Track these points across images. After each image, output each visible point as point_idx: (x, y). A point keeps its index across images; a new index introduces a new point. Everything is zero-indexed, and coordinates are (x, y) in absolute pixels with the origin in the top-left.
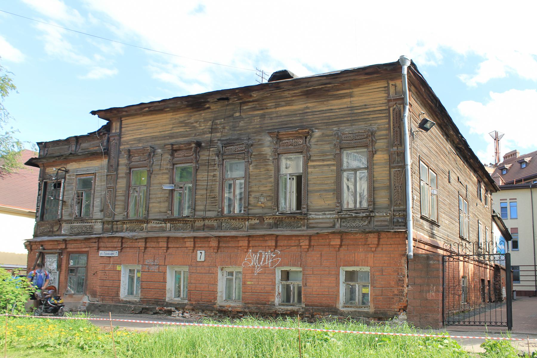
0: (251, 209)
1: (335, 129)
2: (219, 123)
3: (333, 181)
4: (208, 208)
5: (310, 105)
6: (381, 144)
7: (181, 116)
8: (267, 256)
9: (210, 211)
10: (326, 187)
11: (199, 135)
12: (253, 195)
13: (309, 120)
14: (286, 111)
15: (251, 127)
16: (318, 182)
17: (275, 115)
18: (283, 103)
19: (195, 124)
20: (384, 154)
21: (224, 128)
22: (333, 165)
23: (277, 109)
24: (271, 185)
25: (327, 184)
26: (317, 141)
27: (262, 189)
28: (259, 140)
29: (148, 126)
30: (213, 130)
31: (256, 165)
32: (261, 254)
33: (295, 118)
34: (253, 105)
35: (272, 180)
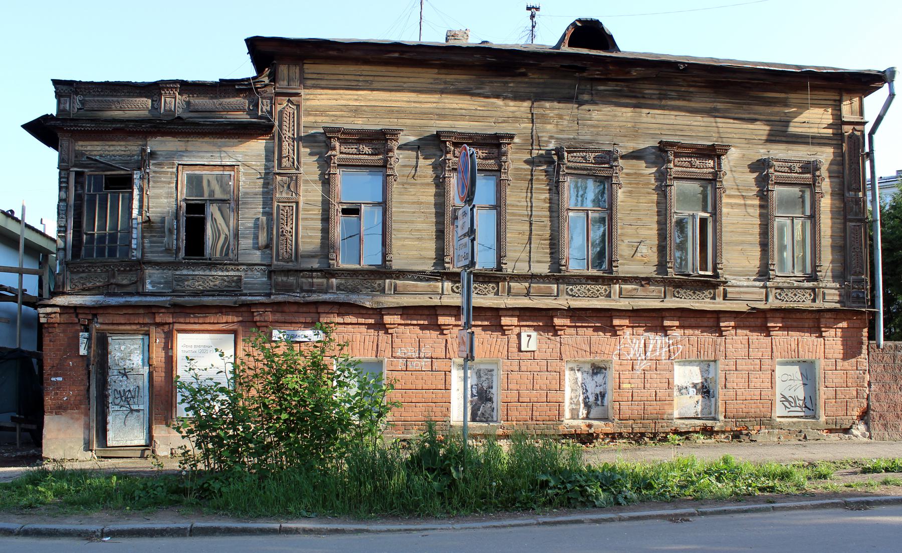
18: (673, 93)
31: (630, 192)
34: (617, 86)
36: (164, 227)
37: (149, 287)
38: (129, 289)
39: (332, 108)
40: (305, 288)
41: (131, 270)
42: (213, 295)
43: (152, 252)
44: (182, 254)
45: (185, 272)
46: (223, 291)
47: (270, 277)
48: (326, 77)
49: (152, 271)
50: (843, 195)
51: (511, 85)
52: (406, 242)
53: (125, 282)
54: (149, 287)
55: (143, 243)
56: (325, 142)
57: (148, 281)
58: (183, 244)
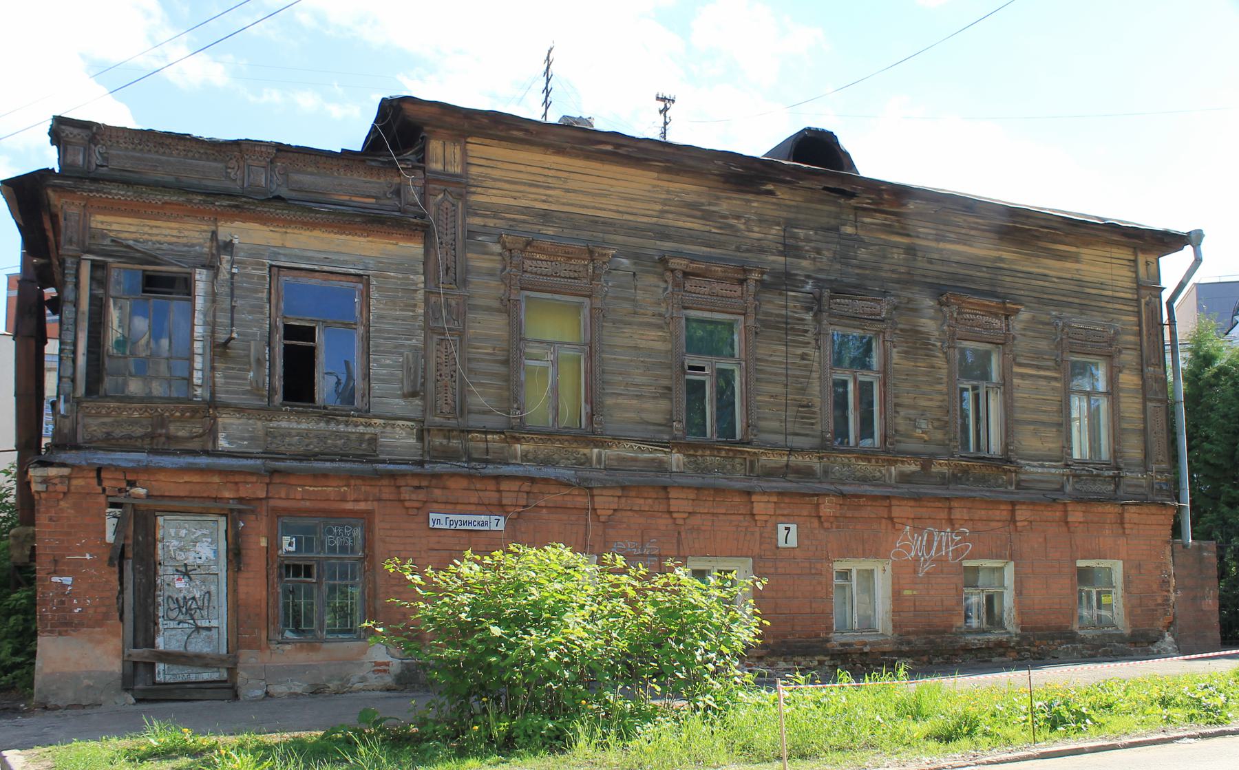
2: (802, 236)
7: (687, 189)
8: (944, 539)
11: (747, 251)
12: (902, 414)
15: (887, 267)
17: (936, 256)
19: (734, 222)
21: (819, 251)
23: (942, 245)
24: (940, 398)
27: (923, 403)
28: (910, 300)
29: (570, 185)
30: (789, 249)
31: (906, 352)
32: (931, 534)
35: (943, 387)
36: (249, 356)
37: (223, 444)
38: (195, 445)
39: (509, 209)
40: (476, 456)
41: (192, 417)
42: (332, 461)
43: (227, 392)
44: (278, 398)
45: (284, 424)
46: (348, 455)
47: (420, 438)
48: (499, 165)
49: (227, 421)
50: (1142, 370)
51: (755, 204)
52: (620, 400)
53: (181, 433)
54: (223, 444)
55: (214, 377)
56: (500, 254)
57: (221, 435)
58: (279, 383)
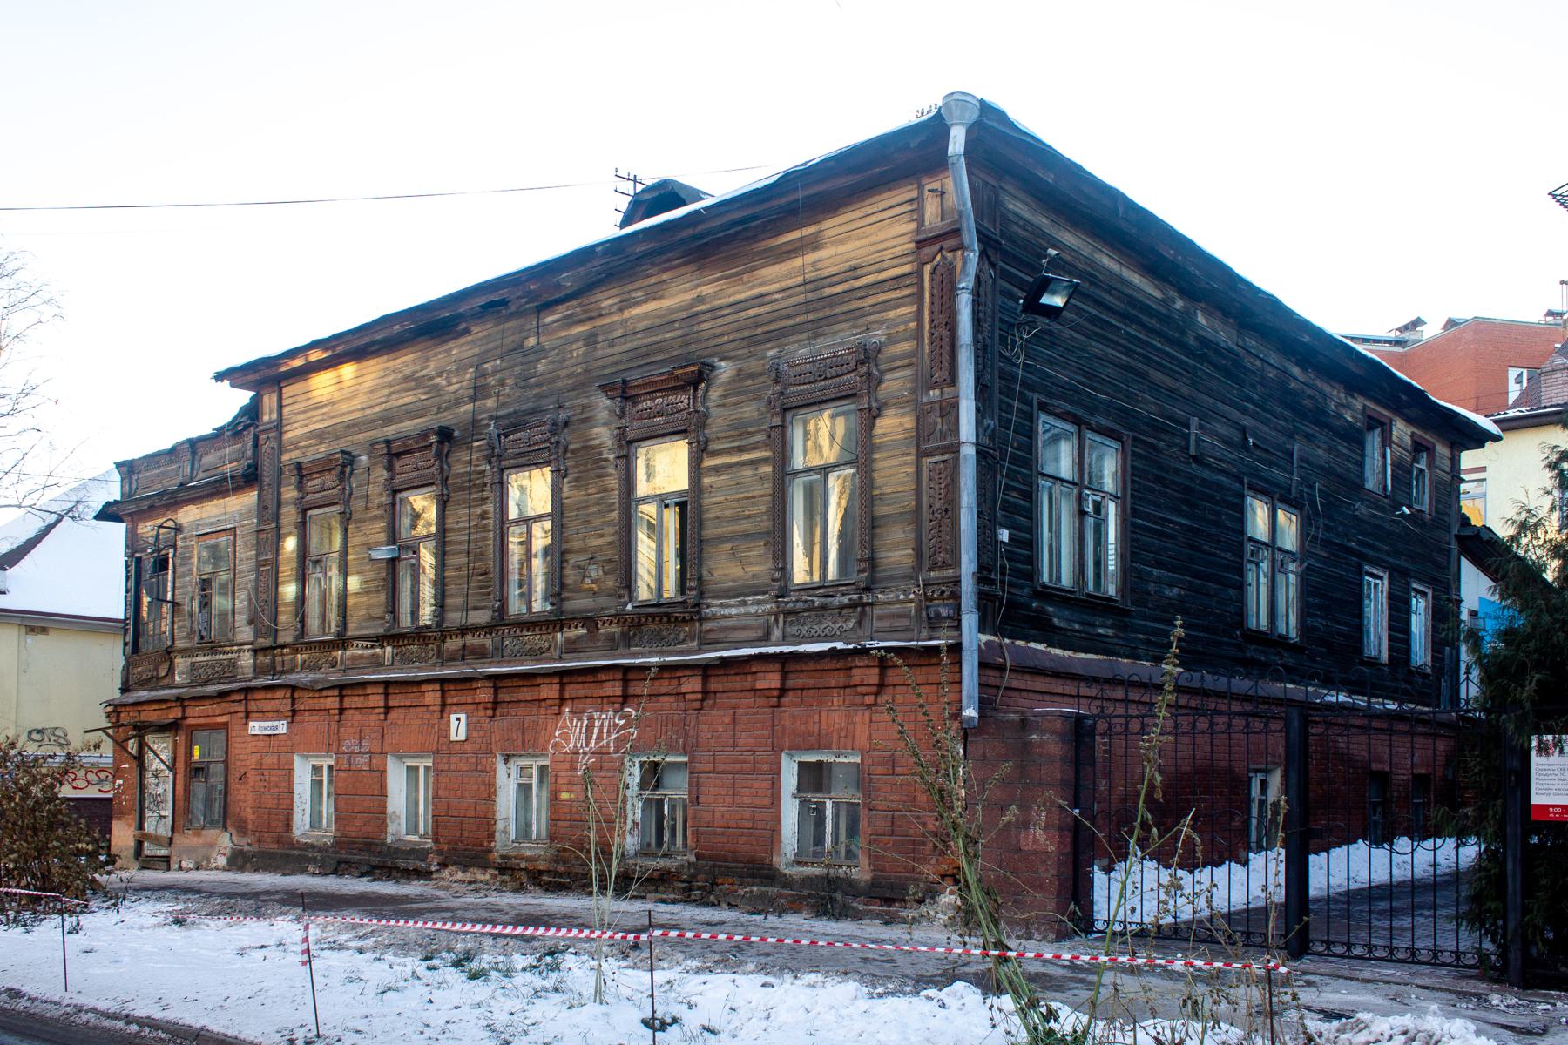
0: (568, 599)
1: (770, 353)
3: (763, 508)
4: (472, 601)
5: (706, 290)
6: (895, 383)
9: (476, 608)
10: (747, 526)
13: (705, 335)
14: (646, 316)
16: (728, 513)
20: (902, 415)
22: (765, 461)
25: (749, 517)
26: (725, 396)
33: (668, 336)
